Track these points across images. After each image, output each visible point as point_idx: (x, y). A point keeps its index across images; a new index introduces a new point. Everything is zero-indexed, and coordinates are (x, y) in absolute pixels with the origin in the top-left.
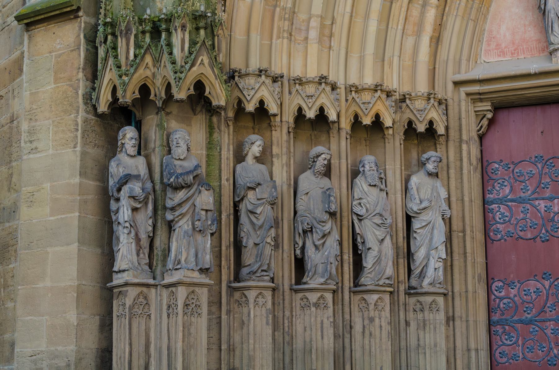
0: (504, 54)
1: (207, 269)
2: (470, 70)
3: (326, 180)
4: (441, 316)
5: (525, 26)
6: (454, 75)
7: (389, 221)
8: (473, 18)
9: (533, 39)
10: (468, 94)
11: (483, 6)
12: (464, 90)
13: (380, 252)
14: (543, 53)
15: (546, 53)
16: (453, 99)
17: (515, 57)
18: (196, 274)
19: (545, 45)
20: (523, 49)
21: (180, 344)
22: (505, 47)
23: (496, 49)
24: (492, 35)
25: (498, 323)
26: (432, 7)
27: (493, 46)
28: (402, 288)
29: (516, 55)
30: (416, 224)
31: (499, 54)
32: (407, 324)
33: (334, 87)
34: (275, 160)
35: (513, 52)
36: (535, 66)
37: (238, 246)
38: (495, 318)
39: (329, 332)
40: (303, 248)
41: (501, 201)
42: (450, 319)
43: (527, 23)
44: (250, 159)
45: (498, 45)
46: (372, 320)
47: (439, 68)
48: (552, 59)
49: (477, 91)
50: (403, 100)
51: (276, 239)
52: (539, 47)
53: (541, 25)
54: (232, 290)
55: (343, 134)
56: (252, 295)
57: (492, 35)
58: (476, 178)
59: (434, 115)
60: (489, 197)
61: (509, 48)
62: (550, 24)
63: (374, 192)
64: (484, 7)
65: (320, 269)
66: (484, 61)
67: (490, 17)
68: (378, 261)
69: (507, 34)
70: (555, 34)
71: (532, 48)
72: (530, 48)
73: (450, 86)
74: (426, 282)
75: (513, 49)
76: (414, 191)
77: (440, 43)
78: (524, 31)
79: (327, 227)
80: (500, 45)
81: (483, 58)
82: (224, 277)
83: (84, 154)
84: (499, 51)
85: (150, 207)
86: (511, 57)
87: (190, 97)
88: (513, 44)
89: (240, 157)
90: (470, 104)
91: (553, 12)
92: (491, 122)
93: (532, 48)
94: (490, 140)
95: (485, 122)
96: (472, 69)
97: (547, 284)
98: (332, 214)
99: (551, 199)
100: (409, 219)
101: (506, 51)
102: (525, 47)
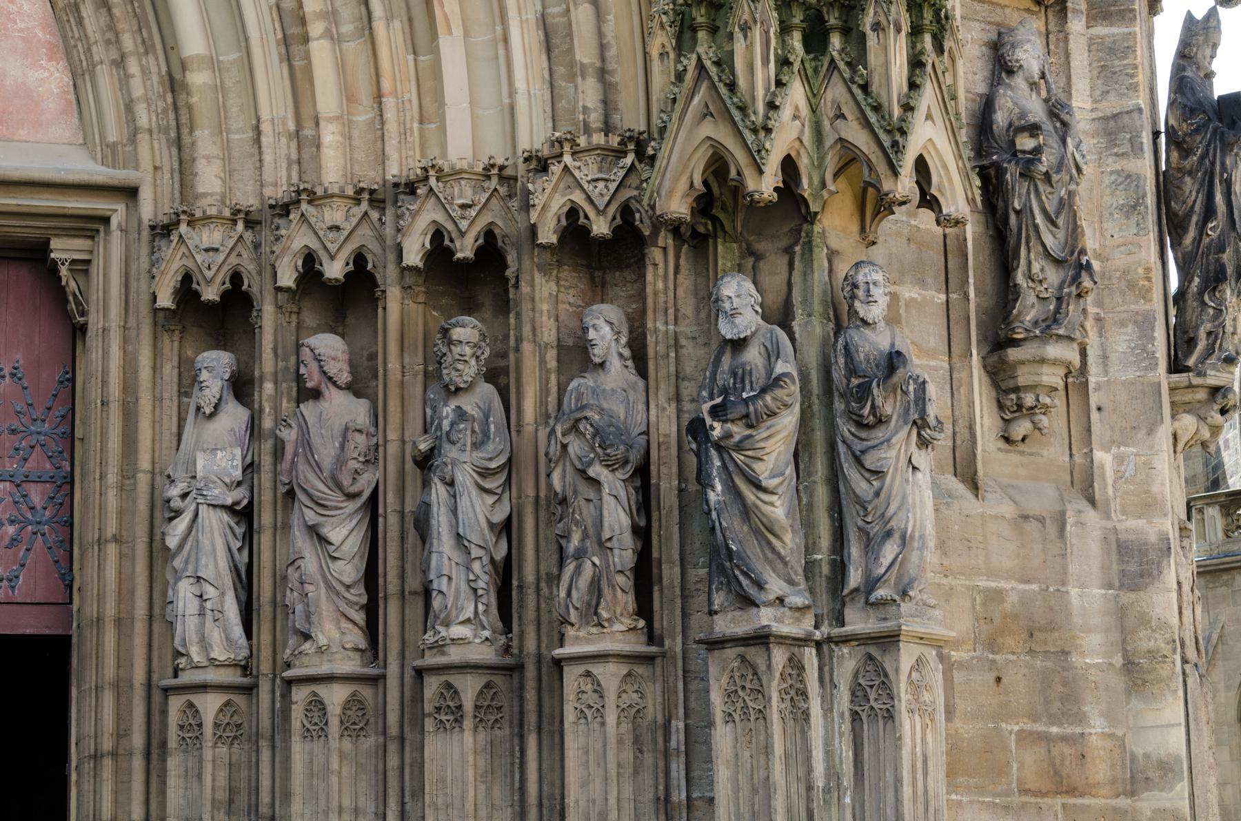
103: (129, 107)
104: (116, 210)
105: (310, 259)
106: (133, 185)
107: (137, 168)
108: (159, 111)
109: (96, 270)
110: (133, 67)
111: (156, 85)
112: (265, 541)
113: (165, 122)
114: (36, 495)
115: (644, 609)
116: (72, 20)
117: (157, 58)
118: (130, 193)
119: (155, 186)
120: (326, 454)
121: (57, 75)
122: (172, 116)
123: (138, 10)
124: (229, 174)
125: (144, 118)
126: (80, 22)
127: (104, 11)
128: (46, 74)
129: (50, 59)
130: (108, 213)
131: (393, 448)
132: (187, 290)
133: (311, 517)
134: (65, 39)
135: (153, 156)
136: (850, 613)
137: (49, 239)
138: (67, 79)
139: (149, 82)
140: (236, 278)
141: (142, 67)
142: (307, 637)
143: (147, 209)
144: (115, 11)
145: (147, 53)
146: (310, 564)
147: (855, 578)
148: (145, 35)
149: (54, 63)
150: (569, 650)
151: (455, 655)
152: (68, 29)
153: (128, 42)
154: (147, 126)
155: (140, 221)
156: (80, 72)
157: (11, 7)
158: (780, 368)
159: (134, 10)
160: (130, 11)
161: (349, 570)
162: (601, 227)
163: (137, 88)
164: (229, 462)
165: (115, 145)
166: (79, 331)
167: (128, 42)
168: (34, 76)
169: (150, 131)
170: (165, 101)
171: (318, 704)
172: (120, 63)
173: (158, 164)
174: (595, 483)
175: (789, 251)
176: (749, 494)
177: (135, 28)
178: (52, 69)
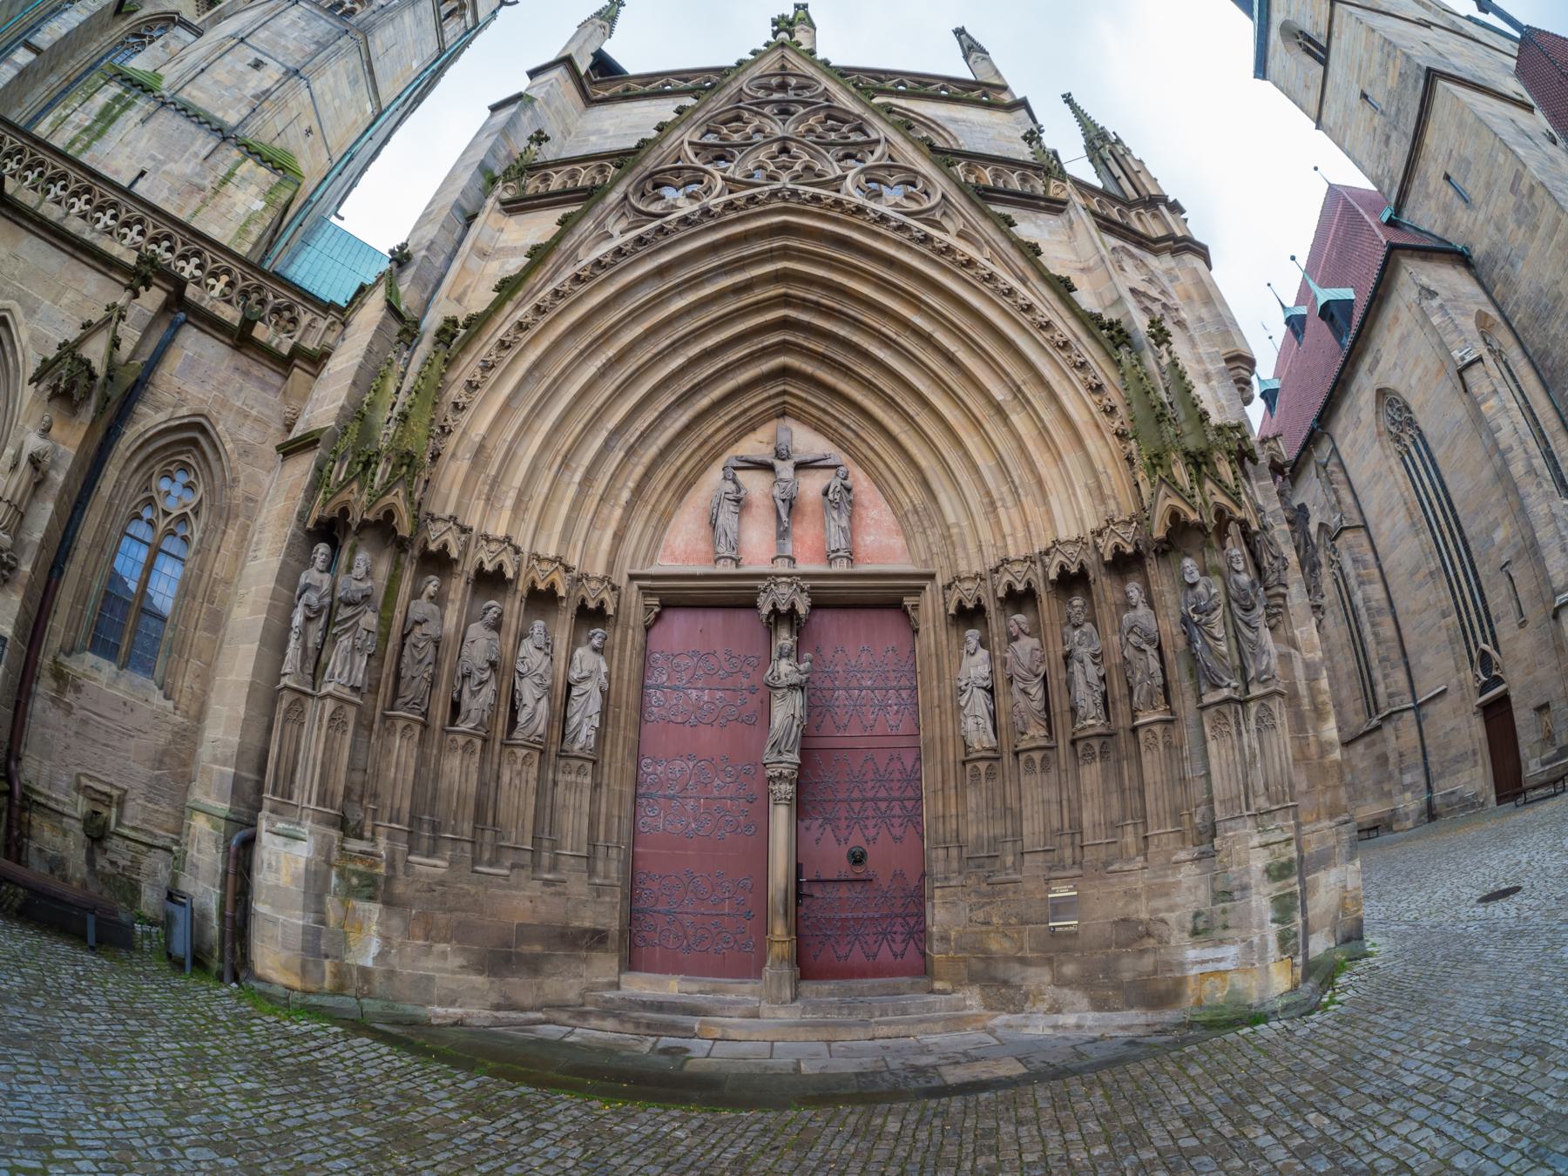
1: (358, 689)
3: (494, 635)
4: (588, 780)
7: (549, 682)
10: (640, 588)
12: (636, 583)
13: (535, 709)
18: (347, 690)
21: (320, 755)
25: (643, 796)
28: (554, 749)
30: (575, 692)
32: (555, 783)
33: (517, 551)
34: (449, 605)
37: (398, 677)
38: (641, 791)
39: (474, 777)
40: (460, 693)
41: (658, 687)
42: (596, 786)
44: (424, 596)
45: (672, 553)
46: (519, 773)
50: (579, 580)
51: (433, 676)
54: (385, 717)
55: (519, 596)
56: (400, 724)
58: (637, 663)
59: (606, 596)
60: (649, 682)
63: (540, 655)
65: (473, 714)
68: (531, 719)
73: (625, 577)
74: (577, 746)
76: (577, 662)
79: (485, 676)
82: (379, 704)
83: (284, 564)
85: (323, 620)
87: (378, 522)
89: (416, 594)
92: (658, 616)
94: (655, 632)
95: (652, 616)
97: (691, 764)
98: (493, 665)
99: (702, 689)
100: (569, 687)
103: (929, 547)
105: (1010, 585)
109: (921, 608)
112: (1001, 700)
114: (904, 694)
115: (1168, 701)
118: (931, 577)
120: (1026, 660)
124: (969, 564)
125: (935, 550)
131: (1052, 656)
132: (961, 607)
133: (1022, 685)
136: (1251, 689)
140: (979, 600)
142: (1023, 734)
143: (939, 581)
146: (1022, 705)
147: (1252, 673)
150: (1140, 721)
151: (1090, 732)
153: (926, 524)
158: (1213, 591)
161: (1038, 705)
162: (1129, 550)
164: (984, 670)
166: (916, 631)
167: (926, 524)
171: (1031, 760)
174: (1144, 651)
175: (1202, 550)
176: (1211, 642)
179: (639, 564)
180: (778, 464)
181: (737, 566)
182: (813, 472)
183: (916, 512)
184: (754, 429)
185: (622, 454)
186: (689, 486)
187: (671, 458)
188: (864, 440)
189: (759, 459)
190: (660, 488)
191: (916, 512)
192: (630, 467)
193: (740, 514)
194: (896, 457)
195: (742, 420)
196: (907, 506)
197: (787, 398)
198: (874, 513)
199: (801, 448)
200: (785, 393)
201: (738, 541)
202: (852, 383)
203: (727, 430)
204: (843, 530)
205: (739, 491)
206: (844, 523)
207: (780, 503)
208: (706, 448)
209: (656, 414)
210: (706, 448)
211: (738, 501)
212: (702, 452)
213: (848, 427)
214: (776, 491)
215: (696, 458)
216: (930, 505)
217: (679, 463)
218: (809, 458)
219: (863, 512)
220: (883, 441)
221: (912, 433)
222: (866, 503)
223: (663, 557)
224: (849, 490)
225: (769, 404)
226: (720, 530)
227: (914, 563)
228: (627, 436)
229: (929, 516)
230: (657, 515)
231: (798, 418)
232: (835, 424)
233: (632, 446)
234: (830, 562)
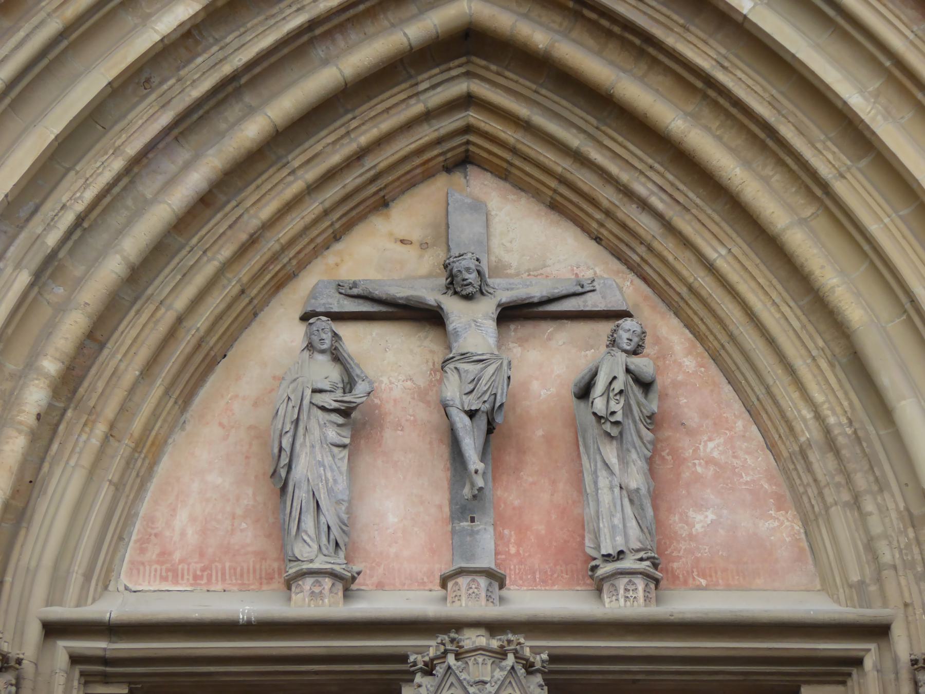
0: (176, 576)
2: (90, 600)
5: (234, 518)
6: (47, 606)
8: (115, 480)
9: (250, 549)
10: (75, 659)
11: (143, 456)
12: (64, 646)
14: (268, 583)
15: (278, 584)
16: (36, 664)
17: (201, 585)
19: (275, 565)
20: (223, 569)
22: (182, 561)
23: (158, 562)
24: (152, 528)
26: (20, 432)
27: (152, 553)
29: (204, 581)
31: (164, 574)
35: (199, 573)
36: (247, 607)
43: (239, 512)
45: (164, 554)
47: (12, 583)
48: (290, 599)
49: (101, 653)
52: (261, 569)
53: (271, 520)
57: (152, 528)
61: (189, 564)
62: (296, 514)
64: (144, 459)
66: (126, 588)
67: (153, 487)
69: (190, 532)
70: (306, 537)
71: (245, 570)
72: (238, 570)
73: (34, 631)
75: (199, 566)
77: (24, 524)
78: (230, 528)
80: (170, 554)
81: (124, 580)
84: (164, 567)
86: (192, 585)
88: (202, 555)
90: (76, 683)
91: (304, 487)
93: (245, 570)
96: (94, 600)
101: (183, 570)
102: (227, 565)
103: (870, 546)
104: (869, 650)
106: (885, 622)
107: (885, 604)
108: (902, 546)
110: (869, 506)
111: (895, 522)
113: (909, 558)
116: (799, 467)
117: (893, 496)
119: (908, 623)
121: (787, 523)
122: (916, 550)
123: (867, 450)
125: (887, 555)
126: (809, 468)
127: (830, 456)
128: (776, 524)
129: (779, 509)
130: (861, 654)
134: (792, 487)
135: (902, 593)
137: (799, 687)
138: (798, 527)
139: (887, 520)
141: (878, 505)
144: (845, 452)
145: (881, 490)
148: (878, 473)
149: (783, 512)
152: (796, 477)
153: (861, 481)
154: (891, 563)
155: (896, 660)
156: (812, 517)
157: (735, 462)
159: (863, 450)
160: (858, 451)
163: (876, 525)
165: (862, 583)
168: (765, 526)
169: (895, 567)
170: (907, 536)
172: (856, 502)
173: (908, 601)
177: (867, 467)
178: (782, 518)
179: (73, 589)
180: (453, 308)
181: (348, 594)
182: (548, 328)
183: (831, 444)
184: (383, 204)
185: (24, 279)
186: (210, 365)
187: (161, 286)
188: (686, 243)
189: (401, 292)
190: (131, 373)
191: (831, 444)
192: (44, 313)
193: (352, 449)
194: (778, 291)
195: (351, 180)
196: (809, 431)
197: (474, 117)
198: (713, 447)
199: (512, 259)
200: (468, 101)
201: (346, 526)
202: (659, 79)
203: (313, 208)
204: (633, 497)
205: (349, 384)
206: (636, 479)
207: (461, 421)
208: (255, 260)
209: (118, 165)
210: (255, 260)
211: (345, 412)
212: (245, 270)
213: (644, 205)
214: (453, 390)
215: (230, 287)
216: (872, 431)
217: (180, 303)
218: (537, 292)
219: (686, 445)
220: (740, 246)
221: (822, 224)
222: (692, 417)
223: (136, 566)
224: (646, 385)
225: (427, 133)
226: (302, 495)
227: (827, 588)
228: (36, 225)
229: (872, 464)
230: (122, 450)
231: (503, 174)
232: (606, 195)
233: (52, 256)
234: (599, 587)
